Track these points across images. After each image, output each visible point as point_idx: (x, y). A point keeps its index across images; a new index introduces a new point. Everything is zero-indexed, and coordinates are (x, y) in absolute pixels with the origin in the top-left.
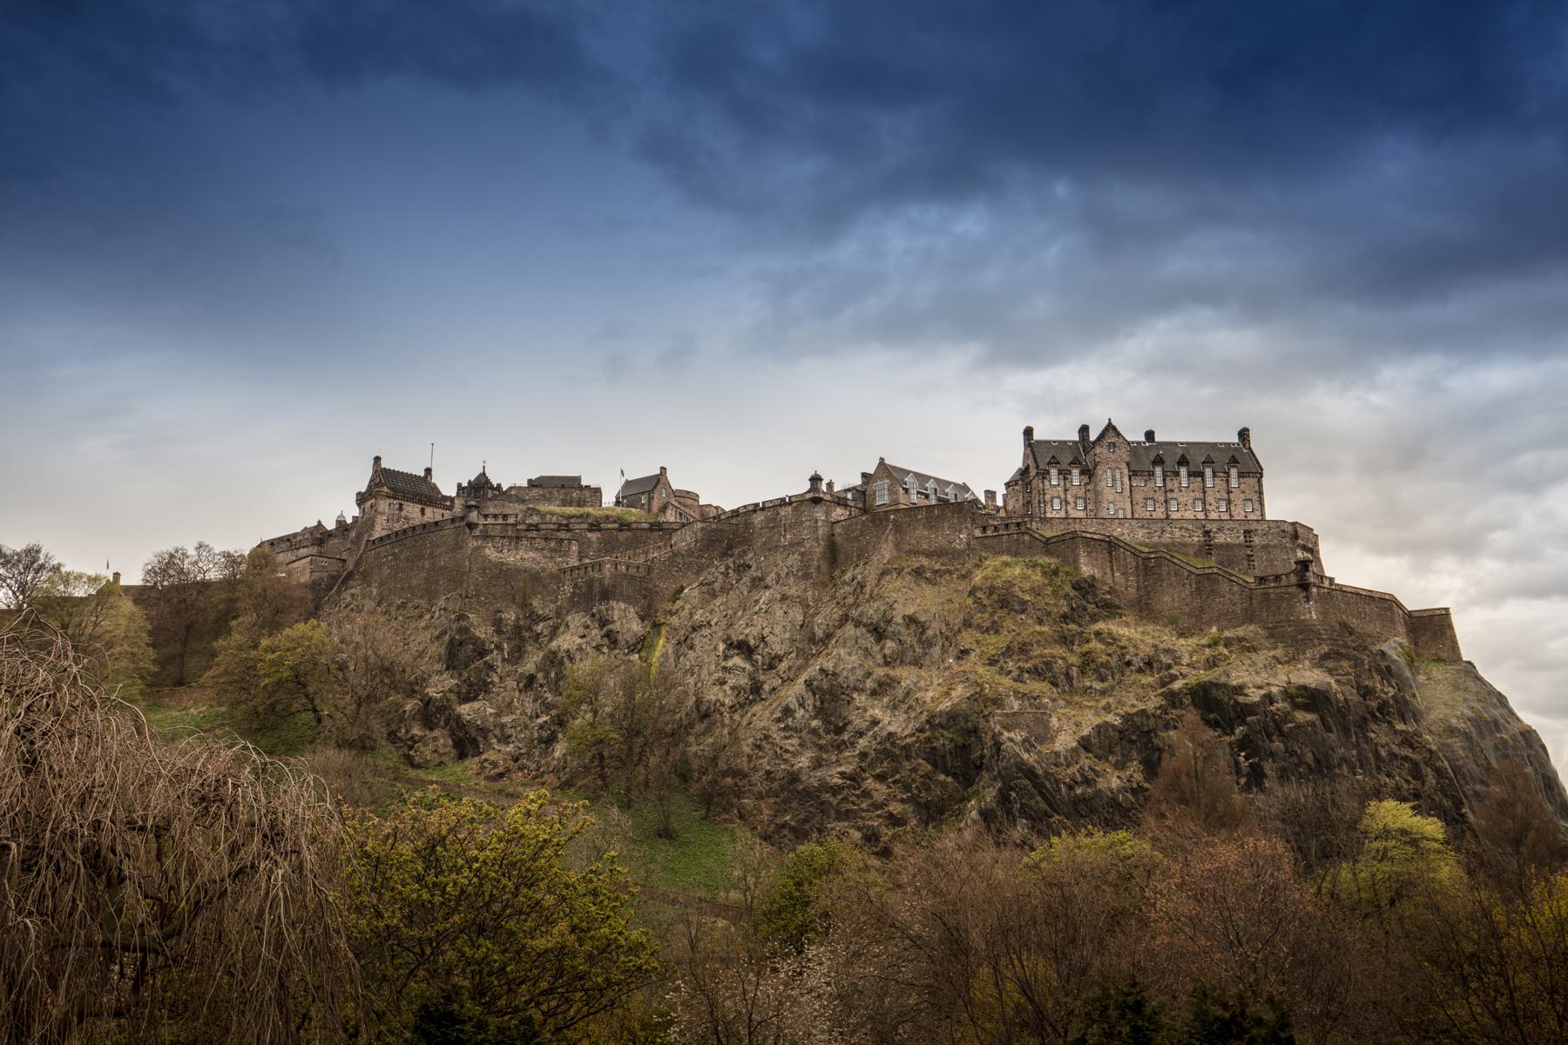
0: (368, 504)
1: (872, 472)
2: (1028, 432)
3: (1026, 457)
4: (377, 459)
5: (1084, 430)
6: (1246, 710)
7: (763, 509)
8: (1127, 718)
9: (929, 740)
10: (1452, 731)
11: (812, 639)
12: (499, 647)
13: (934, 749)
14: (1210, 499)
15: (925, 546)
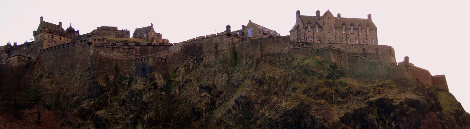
0: (39, 35)
1: (246, 25)
2: (298, 12)
3: (297, 21)
4: (42, 18)
5: (318, 12)
6: (394, 107)
7: (207, 38)
8: (355, 111)
9: (285, 120)
10: (451, 114)
11: (233, 85)
12: (109, 90)
13: (288, 123)
14: (361, 38)
15: (272, 52)
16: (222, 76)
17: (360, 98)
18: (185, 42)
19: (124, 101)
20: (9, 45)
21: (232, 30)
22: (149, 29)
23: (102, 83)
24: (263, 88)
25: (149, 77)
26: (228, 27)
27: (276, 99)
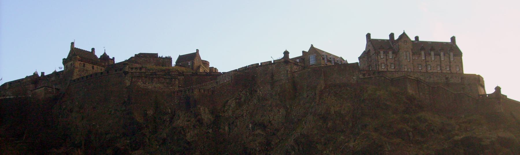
0: (69, 64)
1: (307, 51)
2: (368, 36)
3: (368, 46)
4: (73, 44)
5: (392, 35)
15: (338, 82)
16: (279, 111)
17: (442, 137)
18: (236, 70)
19: (164, 140)
20: (36, 74)
21: (291, 56)
22: (195, 56)
23: (139, 119)
24: (327, 124)
25: (193, 112)
26: (286, 53)
27: (342, 137)
